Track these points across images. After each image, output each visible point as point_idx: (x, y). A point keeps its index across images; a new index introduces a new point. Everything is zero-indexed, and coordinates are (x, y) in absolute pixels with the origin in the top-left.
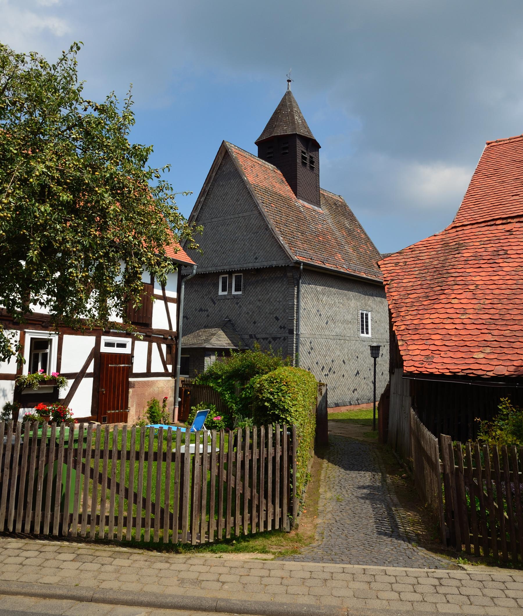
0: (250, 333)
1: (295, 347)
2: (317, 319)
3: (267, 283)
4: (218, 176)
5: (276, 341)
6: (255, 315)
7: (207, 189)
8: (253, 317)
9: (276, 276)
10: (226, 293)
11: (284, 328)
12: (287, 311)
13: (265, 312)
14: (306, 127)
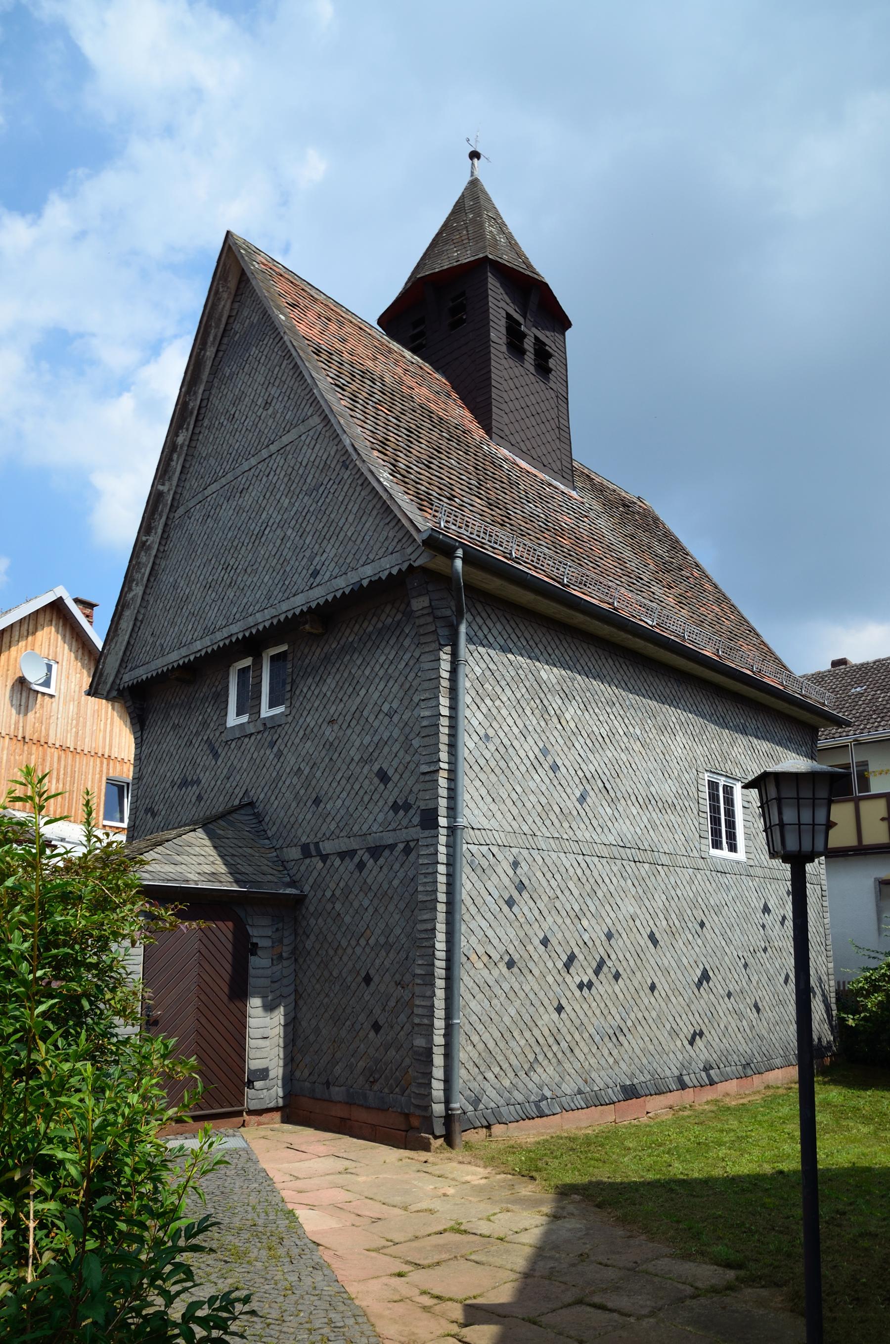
0: (304, 839)
1: (442, 879)
2: (539, 780)
3: (356, 655)
4: (221, 354)
5: (381, 861)
6: (318, 774)
7: (194, 404)
8: (314, 782)
9: (380, 625)
10: (244, 719)
11: (407, 807)
12: (416, 743)
13: (348, 760)
14: (519, 254)
